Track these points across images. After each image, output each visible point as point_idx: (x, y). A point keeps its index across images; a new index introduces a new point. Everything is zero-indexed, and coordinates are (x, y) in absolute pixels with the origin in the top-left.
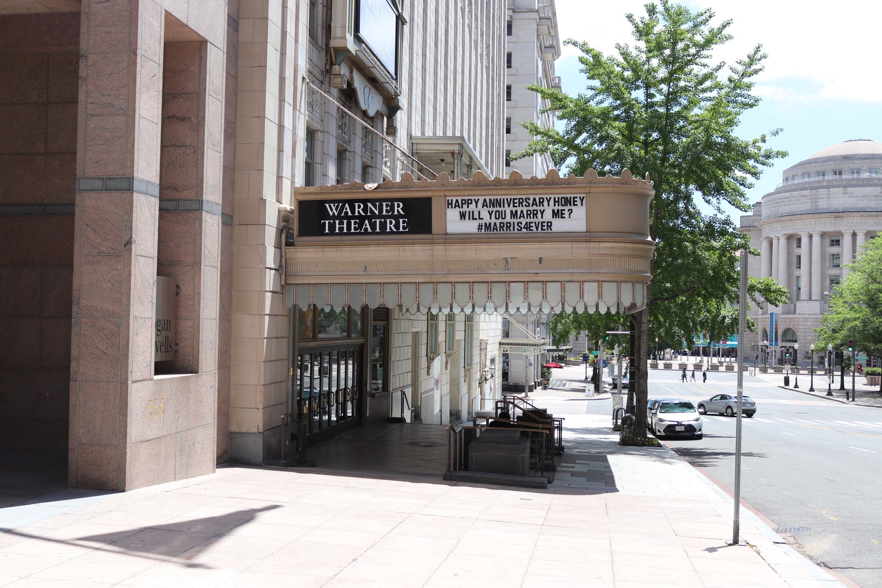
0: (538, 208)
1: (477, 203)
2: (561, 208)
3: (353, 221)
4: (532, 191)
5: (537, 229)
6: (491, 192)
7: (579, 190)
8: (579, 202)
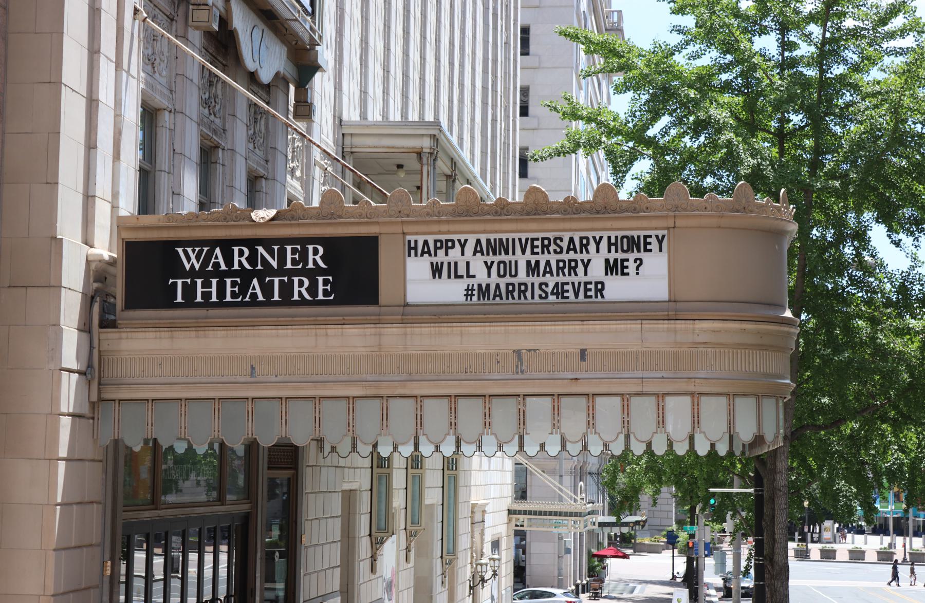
0: (578, 257)
1: (463, 246)
2: (620, 256)
3: (228, 281)
4: (568, 225)
5: (577, 295)
6: (489, 227)
7: (654, 223)
8: (654, 245)
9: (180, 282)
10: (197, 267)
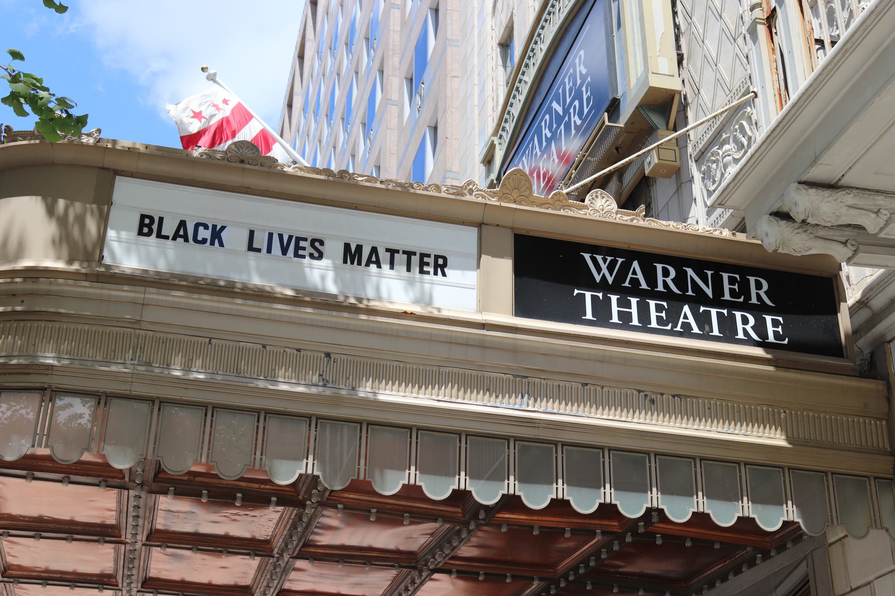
3: (652, 304)
9: (588, 295)
10: (610, 280)
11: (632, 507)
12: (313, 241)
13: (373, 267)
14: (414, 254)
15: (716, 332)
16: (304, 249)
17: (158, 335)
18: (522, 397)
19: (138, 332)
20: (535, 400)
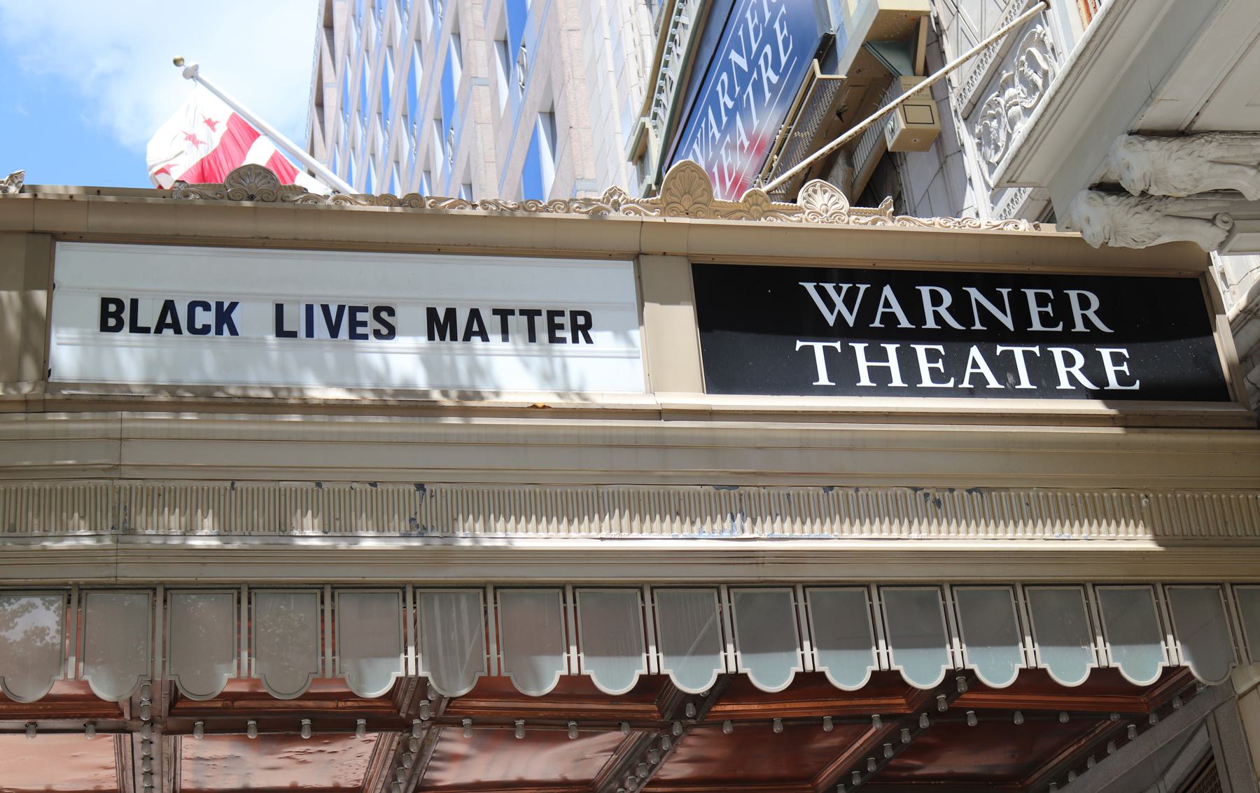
3: (920, 350)
9: (818, 347)
10: (850, 320)
11: (924, 672)
12: (377, 311)
13: (477, 340)
14: (539, 313)
15: (1025, 383)
16: (364, 324)
17: (150, 484)
18: (733, 519)
19: (117, 483)
20: (754, 522)
